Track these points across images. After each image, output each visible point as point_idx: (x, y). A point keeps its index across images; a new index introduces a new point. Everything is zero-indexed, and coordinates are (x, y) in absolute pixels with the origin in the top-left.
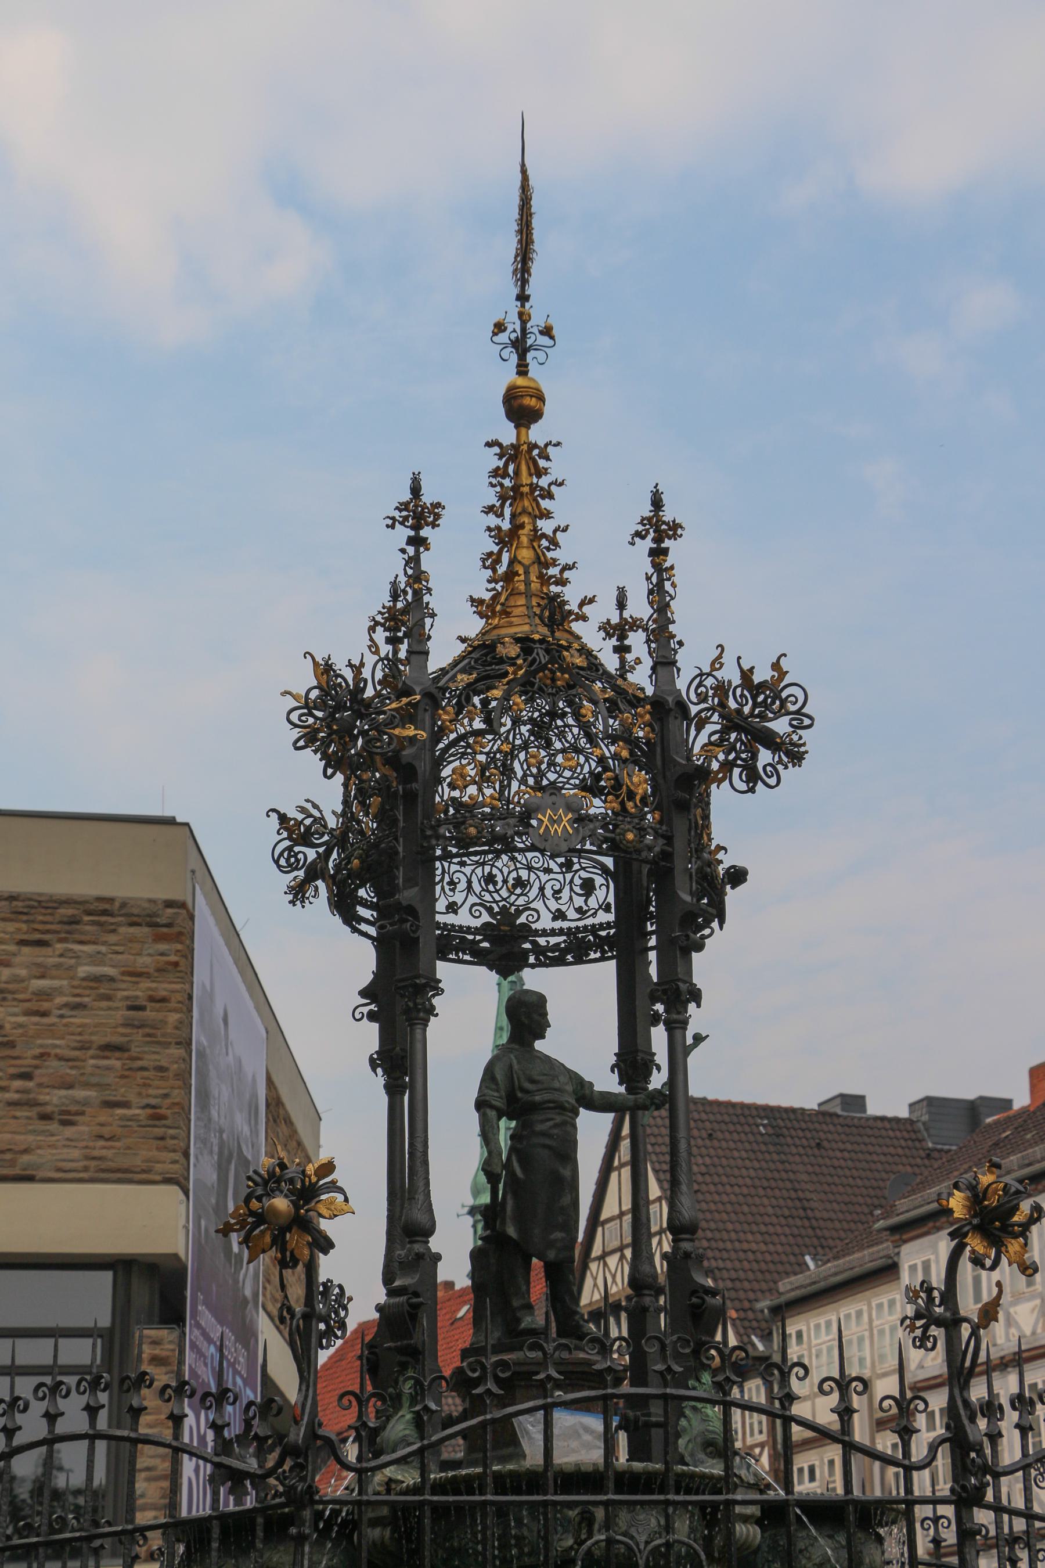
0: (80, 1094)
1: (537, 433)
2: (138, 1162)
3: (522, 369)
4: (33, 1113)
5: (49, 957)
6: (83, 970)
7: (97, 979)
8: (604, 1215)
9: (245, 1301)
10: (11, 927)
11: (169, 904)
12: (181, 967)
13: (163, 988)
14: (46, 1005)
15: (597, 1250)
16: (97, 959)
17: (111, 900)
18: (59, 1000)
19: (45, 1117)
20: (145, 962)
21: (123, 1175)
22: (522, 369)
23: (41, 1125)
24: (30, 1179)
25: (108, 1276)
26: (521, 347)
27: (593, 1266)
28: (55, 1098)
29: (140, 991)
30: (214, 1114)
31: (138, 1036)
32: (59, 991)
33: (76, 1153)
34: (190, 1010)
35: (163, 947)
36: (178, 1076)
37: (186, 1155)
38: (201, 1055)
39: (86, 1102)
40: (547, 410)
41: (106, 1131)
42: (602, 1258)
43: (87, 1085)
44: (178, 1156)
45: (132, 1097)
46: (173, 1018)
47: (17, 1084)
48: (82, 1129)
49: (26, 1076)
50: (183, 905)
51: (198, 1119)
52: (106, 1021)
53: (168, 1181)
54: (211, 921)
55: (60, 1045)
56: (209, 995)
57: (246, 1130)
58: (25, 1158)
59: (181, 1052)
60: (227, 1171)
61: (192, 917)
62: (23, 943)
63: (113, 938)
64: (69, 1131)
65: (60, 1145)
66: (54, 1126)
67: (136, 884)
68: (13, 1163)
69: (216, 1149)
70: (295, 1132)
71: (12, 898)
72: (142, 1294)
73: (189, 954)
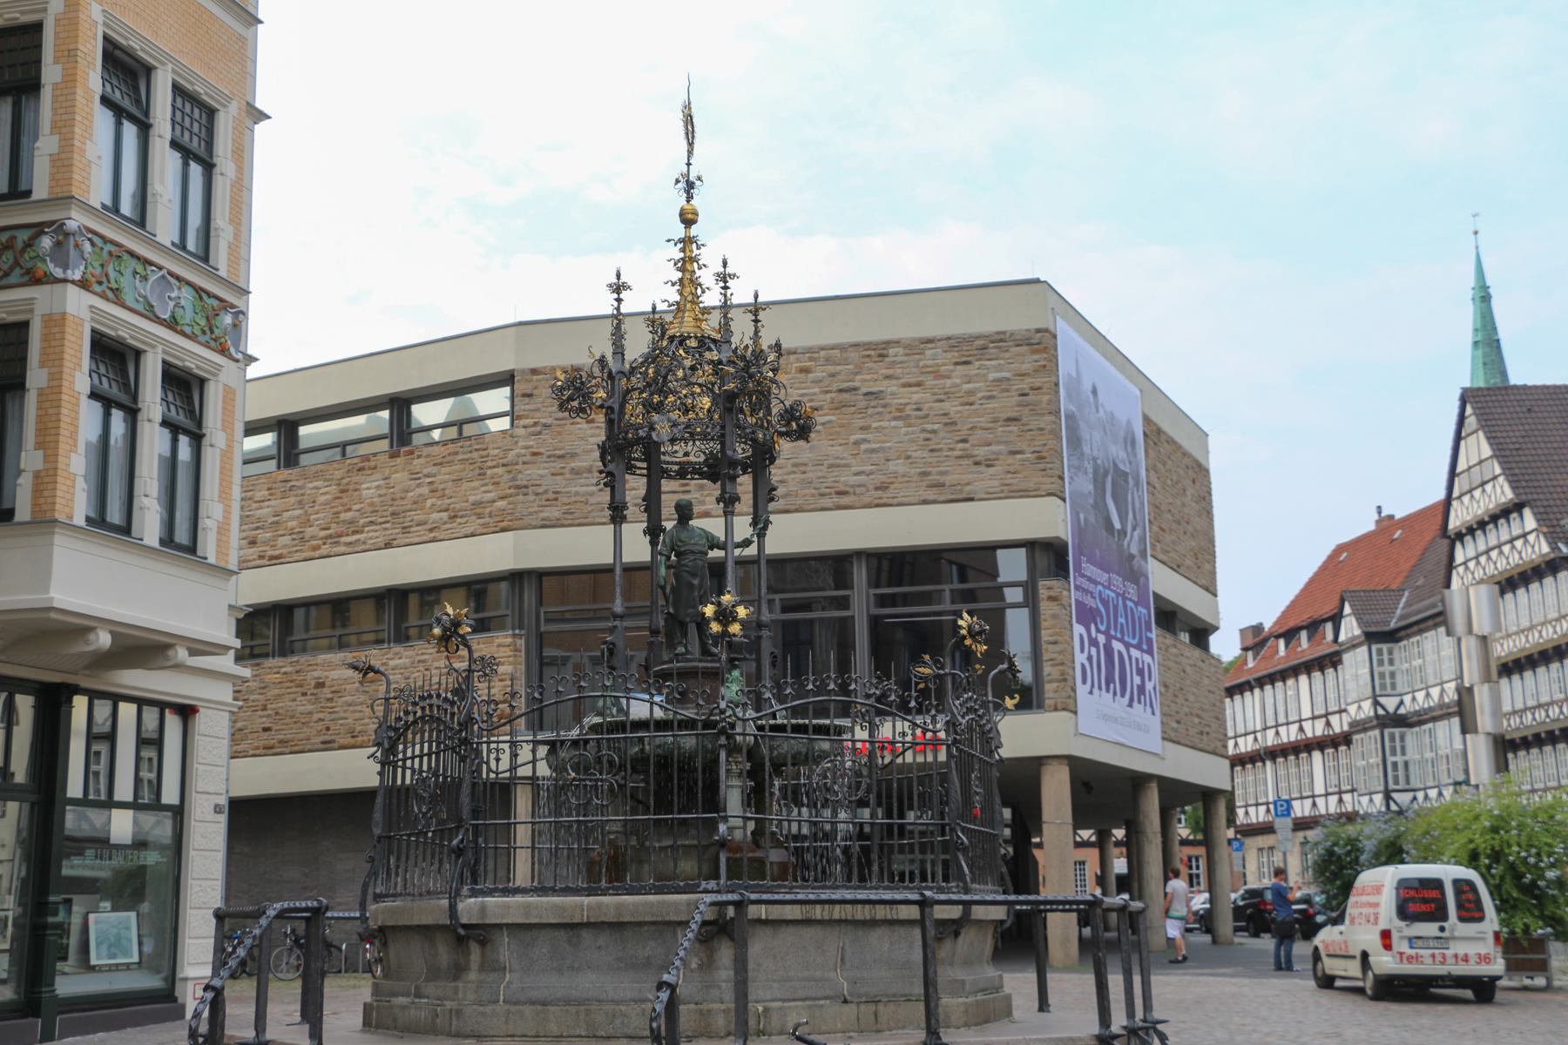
0: (995, 448)
1: (694, 230)
2: (1031, 485)
3: (689, 198)
4: (969, 462)
5: (971, 370)
6: (992, 376)
7: (999, 380)
8: (1459, 470)
9: (1132, 557)
10: (949, 355)
11: (1038, 331)
12: (1050, 365)
13: (1038, 381)
14: (972, 399)
15: (1456, 493)
16: (999, 369)
17: (1004, 333)
18: (980, 395)
19: (977, 463)
20: (1027, 367)
21: (1024, 493)
22: (689, 198)
23: (976, 468)
24: (971, 499)
25: (1023, 550)
26: (690, 186)
27: (1455, 503)
28: (981, 452)
29: (1025, 385)
30: (1087, 450)
31: (1026, 411)
32: (979, 390)
33: (996, 483)
34: (1057, 392)
35: (1036, 357)
36: (1051, 432)
37: (1061, 478)
38: (1071, 417)
39: (998, 453)
40: (700, 219)
41: (1012, 469)
42: (1459, 498)
43: (999, 443)
44: (1055, 479)
45: (1025, 447)
46: (1045, 398)
47: (960, 446)
48: (998, 469)
49: (965, 441)
50: (1046, 331)
51: (1070, 455)
52: (1007, 404)
53: (1049, 495)
54: (1075, 335)
55: (982, 421)
56: (1076, 381)
57: (1122, 454)
58: (968, 488)
59: (1051, 418)
60: (1104, 485)
61: (1055, 337)
62: (957, 364)
63: (1007, 355)
64: (991, 470)
65: (984, 480)
66: (982, 468)
67: (1018, 321)
68: (961, 491)
69: (1090, 470)
70: (1180, 447)
71: (949, 338)
72: (1043, 560)
73: (1054, 359)
